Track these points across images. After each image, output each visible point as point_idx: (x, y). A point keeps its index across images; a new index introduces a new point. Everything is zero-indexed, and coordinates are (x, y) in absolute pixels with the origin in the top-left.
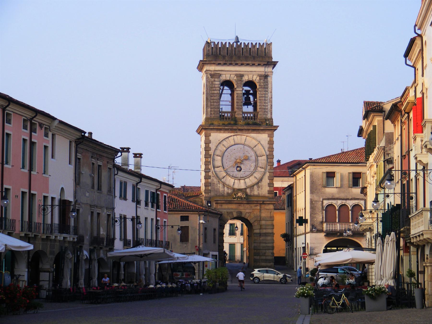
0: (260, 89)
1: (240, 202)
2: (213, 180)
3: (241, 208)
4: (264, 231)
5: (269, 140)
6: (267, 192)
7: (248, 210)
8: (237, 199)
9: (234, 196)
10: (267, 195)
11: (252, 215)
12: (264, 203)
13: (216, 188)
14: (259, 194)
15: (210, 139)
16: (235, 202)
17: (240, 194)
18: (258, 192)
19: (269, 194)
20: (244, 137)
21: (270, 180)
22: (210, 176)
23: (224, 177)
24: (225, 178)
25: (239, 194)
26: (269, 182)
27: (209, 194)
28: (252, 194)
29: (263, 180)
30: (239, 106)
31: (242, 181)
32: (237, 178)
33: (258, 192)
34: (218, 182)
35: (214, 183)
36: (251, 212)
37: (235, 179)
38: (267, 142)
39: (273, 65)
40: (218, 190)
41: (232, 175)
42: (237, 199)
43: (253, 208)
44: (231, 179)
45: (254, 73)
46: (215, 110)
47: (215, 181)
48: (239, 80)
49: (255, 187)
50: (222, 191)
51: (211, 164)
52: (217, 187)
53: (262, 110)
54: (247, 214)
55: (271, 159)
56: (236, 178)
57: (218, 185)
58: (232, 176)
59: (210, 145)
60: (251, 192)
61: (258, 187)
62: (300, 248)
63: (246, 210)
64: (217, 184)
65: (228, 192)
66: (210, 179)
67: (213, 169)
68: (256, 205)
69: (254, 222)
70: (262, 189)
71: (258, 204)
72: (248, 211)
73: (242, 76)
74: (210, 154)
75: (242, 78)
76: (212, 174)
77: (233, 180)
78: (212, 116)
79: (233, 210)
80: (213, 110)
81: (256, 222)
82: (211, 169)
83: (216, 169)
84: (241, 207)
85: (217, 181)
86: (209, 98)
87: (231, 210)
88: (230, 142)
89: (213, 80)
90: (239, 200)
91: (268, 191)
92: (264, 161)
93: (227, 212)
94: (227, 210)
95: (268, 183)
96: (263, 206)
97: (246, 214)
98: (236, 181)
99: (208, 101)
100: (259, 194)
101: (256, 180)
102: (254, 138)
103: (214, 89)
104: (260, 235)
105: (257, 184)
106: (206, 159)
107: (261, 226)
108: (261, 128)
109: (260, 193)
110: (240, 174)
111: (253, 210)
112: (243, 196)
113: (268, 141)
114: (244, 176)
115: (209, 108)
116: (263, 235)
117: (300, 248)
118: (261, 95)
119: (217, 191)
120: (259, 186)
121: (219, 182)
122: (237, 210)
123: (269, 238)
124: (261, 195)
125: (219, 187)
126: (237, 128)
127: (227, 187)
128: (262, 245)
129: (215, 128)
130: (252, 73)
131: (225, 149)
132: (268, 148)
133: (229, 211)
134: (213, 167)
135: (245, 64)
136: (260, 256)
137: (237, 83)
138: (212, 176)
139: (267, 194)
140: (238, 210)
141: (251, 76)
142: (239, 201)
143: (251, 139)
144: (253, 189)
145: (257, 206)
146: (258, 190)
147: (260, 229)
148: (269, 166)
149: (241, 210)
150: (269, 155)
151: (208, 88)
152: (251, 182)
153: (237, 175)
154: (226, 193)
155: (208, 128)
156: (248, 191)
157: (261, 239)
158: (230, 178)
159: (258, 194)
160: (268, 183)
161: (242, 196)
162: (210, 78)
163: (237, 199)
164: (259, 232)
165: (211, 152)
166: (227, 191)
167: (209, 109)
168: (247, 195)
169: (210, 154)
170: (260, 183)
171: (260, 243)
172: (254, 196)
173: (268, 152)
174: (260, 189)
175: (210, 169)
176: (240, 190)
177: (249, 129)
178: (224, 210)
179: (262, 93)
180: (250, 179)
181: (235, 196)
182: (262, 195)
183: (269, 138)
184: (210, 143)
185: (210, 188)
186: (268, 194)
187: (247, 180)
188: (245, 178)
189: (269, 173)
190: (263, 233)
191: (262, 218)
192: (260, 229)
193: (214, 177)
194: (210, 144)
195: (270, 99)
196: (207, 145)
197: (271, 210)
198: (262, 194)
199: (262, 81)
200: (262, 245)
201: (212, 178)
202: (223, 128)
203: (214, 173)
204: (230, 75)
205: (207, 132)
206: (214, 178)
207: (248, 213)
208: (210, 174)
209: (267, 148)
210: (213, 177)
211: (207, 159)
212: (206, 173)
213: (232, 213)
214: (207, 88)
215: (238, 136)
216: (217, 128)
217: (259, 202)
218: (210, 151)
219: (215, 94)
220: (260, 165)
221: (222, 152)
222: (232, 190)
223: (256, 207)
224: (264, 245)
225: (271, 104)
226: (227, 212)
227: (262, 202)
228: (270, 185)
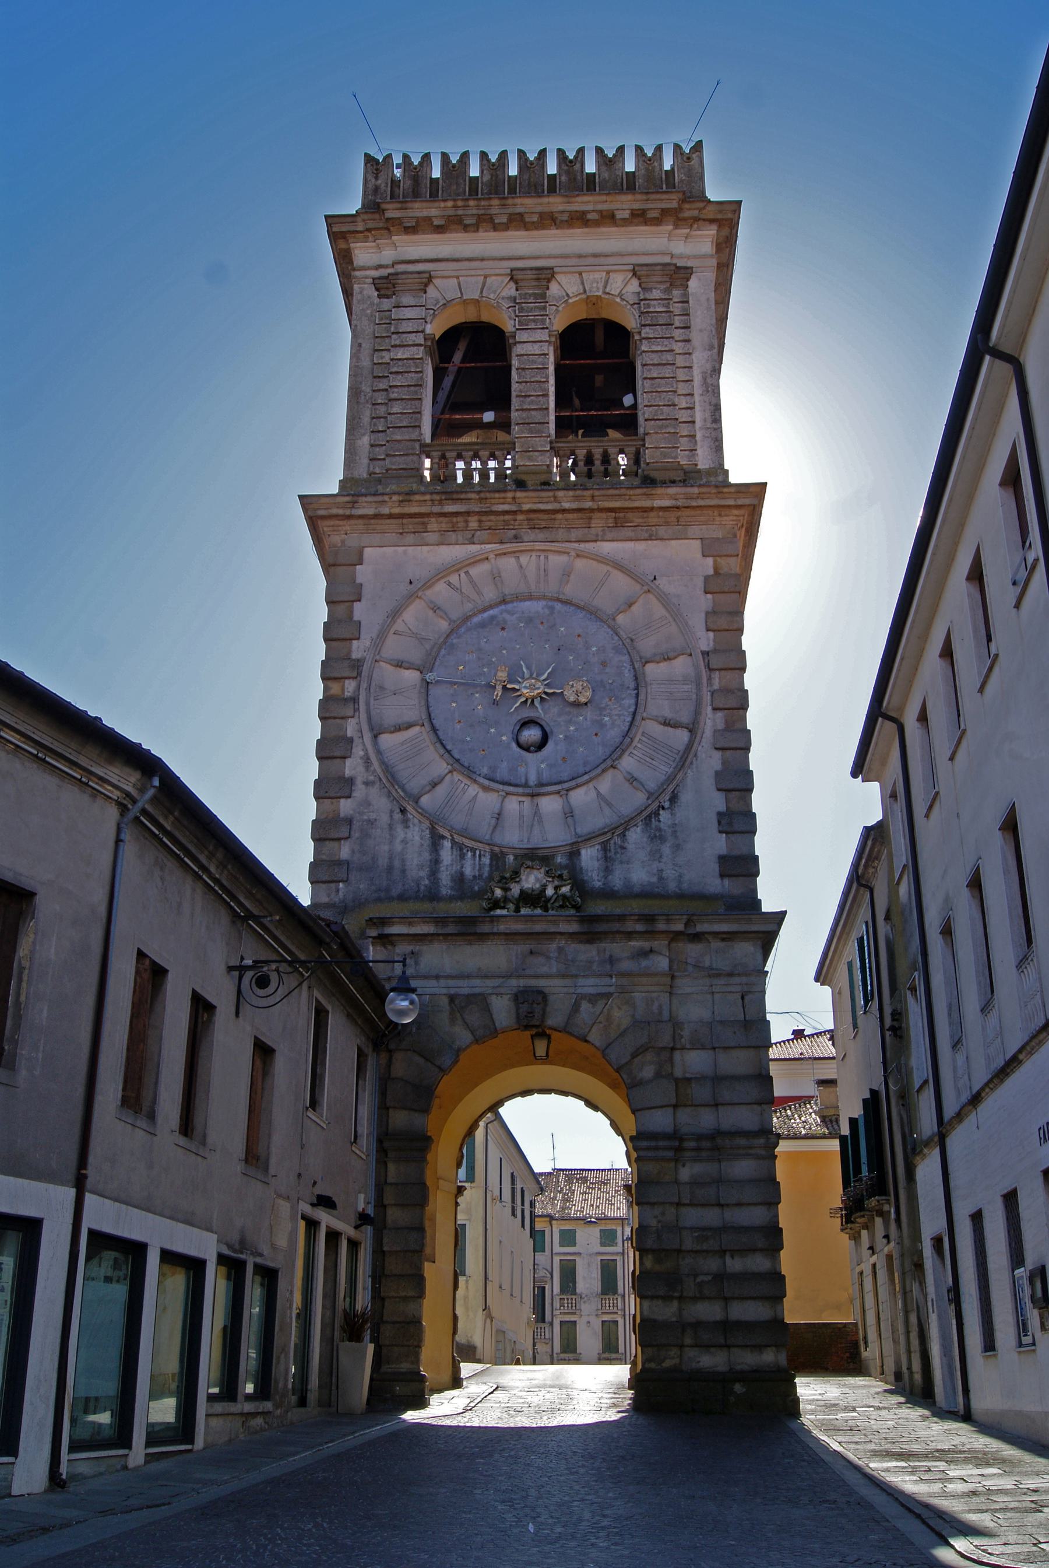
0: (646, 332)
1: (539, 927)
2: (366, 803)
3: (545, 969)
4: (707, 1120)
5: (711, 572)
6: (715, 867)
7: (591, 981)
8: (511, 906)
9: (498, 892)
10: (715, 884)
11: (616, 1014)
12: (700, 928)
13: (386, 848)
14: (661, 879)
15: (358, 581)
16: (502, 927)
17: (537, 880)
18: (655, 866)
19: (726, 881)
20: (556, 561)
21: (728, 791)
22: (351, 781)
23: (434, 785)
24: (441, 790)
25: (531, 880)
26: (723, 808)
27: (338, 890)
28: (617, 881)
29: (686, 797)
30: (533, 413)
31: (550, 805)
32: (516, 786)
33: (655, 866)
34: (398, 816)
35: (371, 823)
36: (607, 996)
37: (508, 794)
38: (700, 582)
39: (712, 221)
40: (397, 863)
41: (485, 770)
42: (517, 910)
43: (626, 965)
44: (482, 795)
45: (611, 260)
46: (399, 438)
47: (381, 805)
48: (530, 295)
49: (635, 835)
50: (421, 867)
51: (356, 710)
52: (391, 842)
53: (667, 427)
54: (585, 1006)
55: (729, 675)
56: (511, 789)
57: (400, 832)
58: (485, 777)
59: (359, 610)
60: (607, 870)
61: (657, 837)
62: (1011, 1199)
63: (581, 981)
64: (391, 827)
65: (462, 874)
66: (349, 797)
67: (367, 737)
68: (646, 945)
69: (634, 1056)
70: (677, 847)
71: (655, 944)
72: (589, 985)
73: (545, 276)
74: (355, 656)
75: (548, 288)
76: (361, 769)
77: (489, 801)
78: (377, 470)
79: (490, 983)
80: (381, 439)
81: (649, 1056)
82: (357, 741)
83: (387, 740)
84: (541, 960)
85: (392, 812)
86: (366, 388)
87: (478, 986)
88: (479, 593)
89: (386, 304)
90: (524, 911)
91: (722, 859)
92: (686, 687)
93: (452, 998)
94: (451, 982)
95: (720, 814)
96: (693, 950)
97: (576, 1008)
98: (513, 805)
99: (362, 399)
100: (661, 879)
101: (639, 798)
102: (618, 566)
103: (395, 340)
104: (679, 1149)
105: (649, 817)
106: (330, 683)
107: (683, 1083)
108: (657, 503)
109: (669, 873)
110: (534, 766)
111: (624, 981)
112: (556, 888)
113: (707, 579)
114: (565, 776)
115: (364, 434)
116: (698, 1149)
117: (1011, 1199)
118: (653, 355)
119: (390, 869)
120: (660, 830)
121: (403, 811)
122: (514, 982)
123: (743, 1168)
124: (672, 886)
125: (404, 842)
126: (514, 508)
127: (454, 843)
128: (693, 1217)
129: (386, 511)
130: (602, 260)
131: (444, 625)
132: (707, 613)
133: (464, 987)
134: (372, 729)
135: (563, 212)
136: (681, 1298)
137: (521, 310)
138: (359, 781)
139: (718, 881)
140: (522, 982)
141: (597, 275)
142: (530, 918)
143: (605, 568)
144: (623, 848)
145: (651, 951)
146: (656, 855)
147: (675, 1107)
148: (720, 714)
149: (541, 983)
150: (715, 651)
151: (367, 346)
152: (607, 811)
153: (522, 770)
154: (445, 878)
155: (348, 512)
156: (589, 857)
157: (685, 1173)
158: (473, 790)
159: (654, 879)
160: (720, 814)
161: (550, 892)
162: (377, 300)
163: (517, 910)
164: (669, 1129)
165: (358, 649)
166: (456, 868)
167: (366, 440)
168: (579, 884)
169: (355, 656)
170: (664, 815)
171: (678, 1204)
172: (630, 894)
173: (711, 634)
174: (666, 850)
175: (351, 740)
176: (534, 857)
177: (592, 510)
178: (434, 982)
179: (659, 348)
180: (599, 794)
181: (506, 889)
182: (685, 886)
183: (710, 561)
184: (360, 601)
185: (345, 851)
186: (722, 876)
187: (580, 797)
188: (566, 786)
189: (718, 755)
190: (700, 1137)
191: (686, 1033)
192: (675, 1107)
193: (373, 783)
194: (357, 606)
195: (705, 379)
196: (341, 609)
197: (744, 979)
198: (680, 882)
199: (656, 294)
200: (693, 1217)
201: (360, 791)
202: (436, 509)
203: (376, 765)
204: (486, 277)
205: (343, 542)
206: (374, 791)
207: (593, 999)
208: (352, 767)
209: (703, 615)
210: (367, 784)
211: (335, 688)
212: (326, 762)
213: (480, 1001)
214: (360, 345)
215: (524, 559)
216: (396, 510)
217: (661, 926)
218: (355, 642)
219: (400, 363)
220: (658, 705)
221: (428, 647)
222: (486, 860)
223: (644, 963)
224: (711, 1217)
225: (714, 401)
226: (452, 998)
227: (679, 927)
228: (730, 824)
